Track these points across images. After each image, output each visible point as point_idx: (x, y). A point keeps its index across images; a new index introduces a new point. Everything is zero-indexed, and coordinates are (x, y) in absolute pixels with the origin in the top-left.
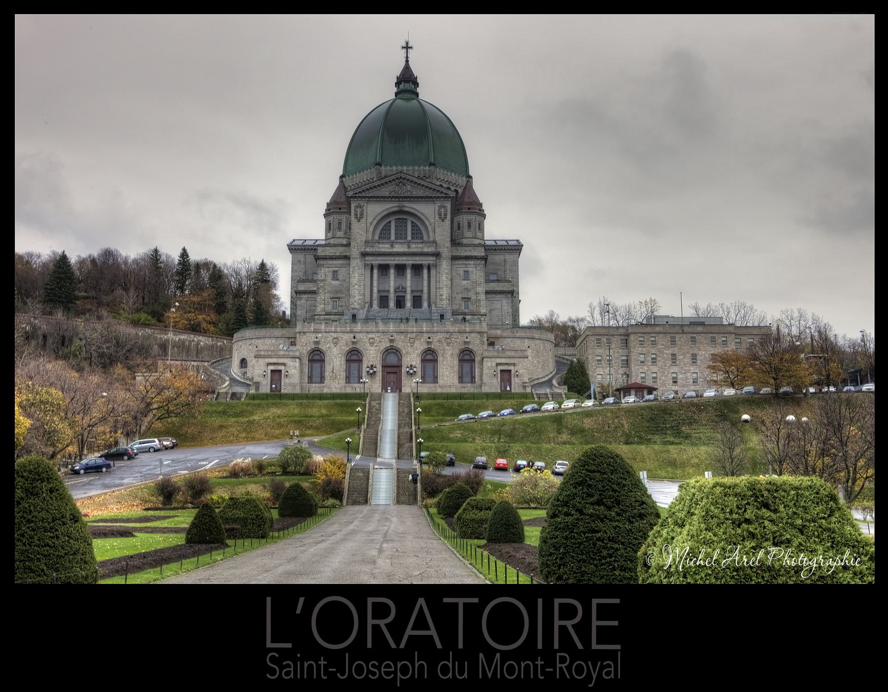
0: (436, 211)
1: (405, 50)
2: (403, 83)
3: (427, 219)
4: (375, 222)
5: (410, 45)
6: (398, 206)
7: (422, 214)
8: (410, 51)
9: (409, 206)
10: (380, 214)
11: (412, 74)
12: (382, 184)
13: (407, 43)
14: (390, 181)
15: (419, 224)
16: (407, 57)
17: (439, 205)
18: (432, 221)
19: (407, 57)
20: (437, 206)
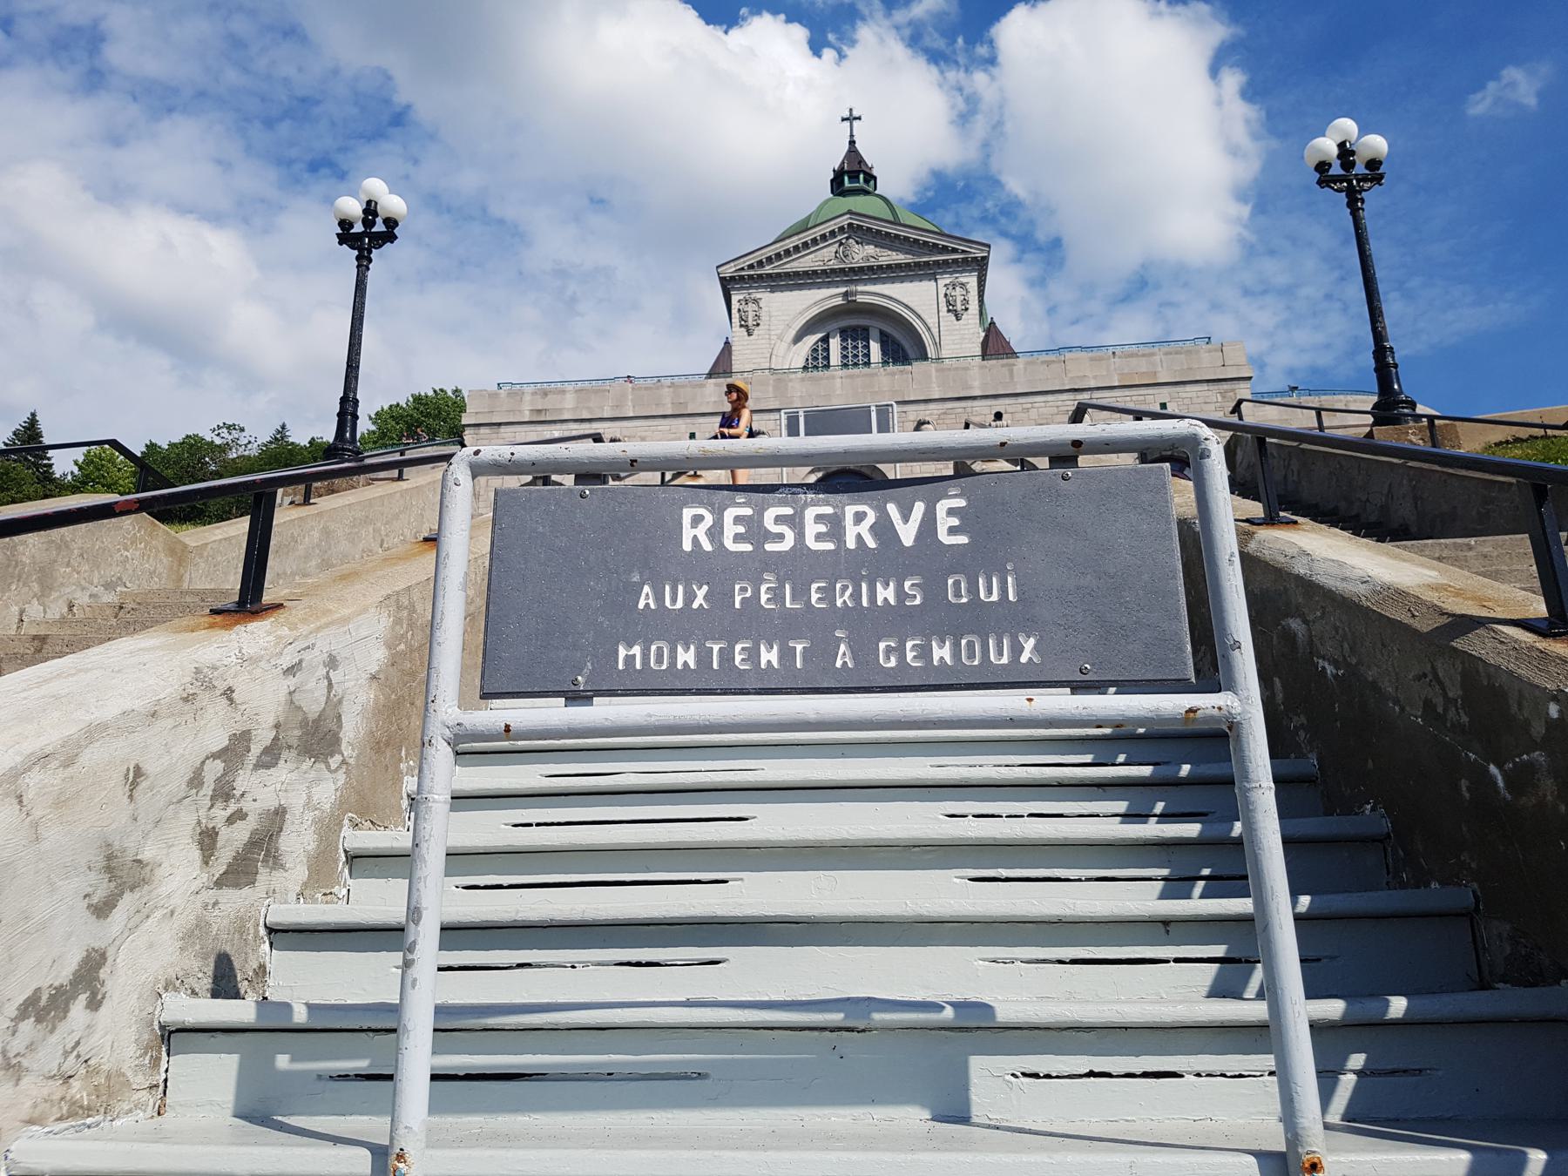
0: (942, 300)
1: (847, 124)
2: (846, 178)
3: (919, 317)
4: (792, 333)
5: (855, 114)
6: (846, 294)
7: (907, 307)
8: (855, 123)
9: (871, 293)
10: (801, 313)
11: (861, 161)
12: (806, 245)
13: (851, 110)
14: (824, 237)
15: (897, 335)
16: (852, 136)
17: (948, 281)
18: (932, 321)
19: (852, 136)
20: (941, 283)
